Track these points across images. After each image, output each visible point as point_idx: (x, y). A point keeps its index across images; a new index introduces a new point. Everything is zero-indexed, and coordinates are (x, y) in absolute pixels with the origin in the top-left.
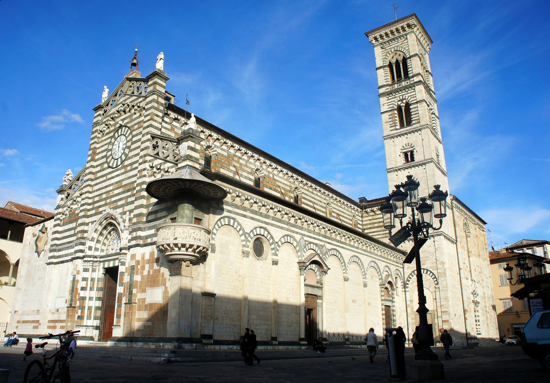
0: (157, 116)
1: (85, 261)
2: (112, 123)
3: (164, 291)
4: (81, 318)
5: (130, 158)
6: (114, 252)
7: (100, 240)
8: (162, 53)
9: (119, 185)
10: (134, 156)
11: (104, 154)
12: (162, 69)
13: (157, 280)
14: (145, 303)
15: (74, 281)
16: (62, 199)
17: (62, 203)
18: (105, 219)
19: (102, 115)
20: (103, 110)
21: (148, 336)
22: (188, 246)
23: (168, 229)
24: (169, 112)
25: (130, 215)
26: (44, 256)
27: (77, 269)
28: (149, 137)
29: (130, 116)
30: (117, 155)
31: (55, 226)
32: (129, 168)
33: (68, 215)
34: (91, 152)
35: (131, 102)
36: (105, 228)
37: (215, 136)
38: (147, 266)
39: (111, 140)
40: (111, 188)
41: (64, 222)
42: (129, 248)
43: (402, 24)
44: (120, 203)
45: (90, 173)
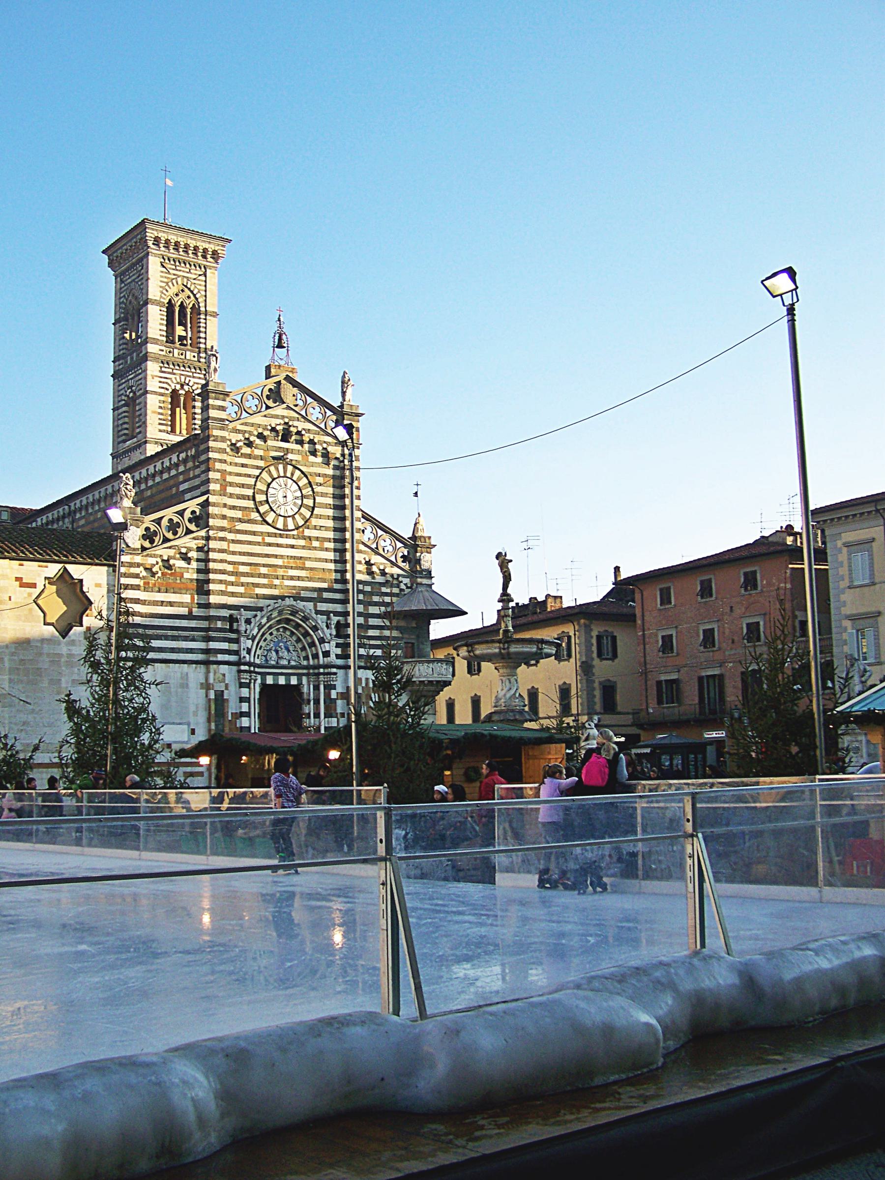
1: (239, 671)
5: (315, 528)
6: (285, 662)
32: (316, 544)
34: (217, 476)
35: (309, 431)
39: (261, 473)
40: (279, 562)
43: (207, 246)
45: (224, 517)
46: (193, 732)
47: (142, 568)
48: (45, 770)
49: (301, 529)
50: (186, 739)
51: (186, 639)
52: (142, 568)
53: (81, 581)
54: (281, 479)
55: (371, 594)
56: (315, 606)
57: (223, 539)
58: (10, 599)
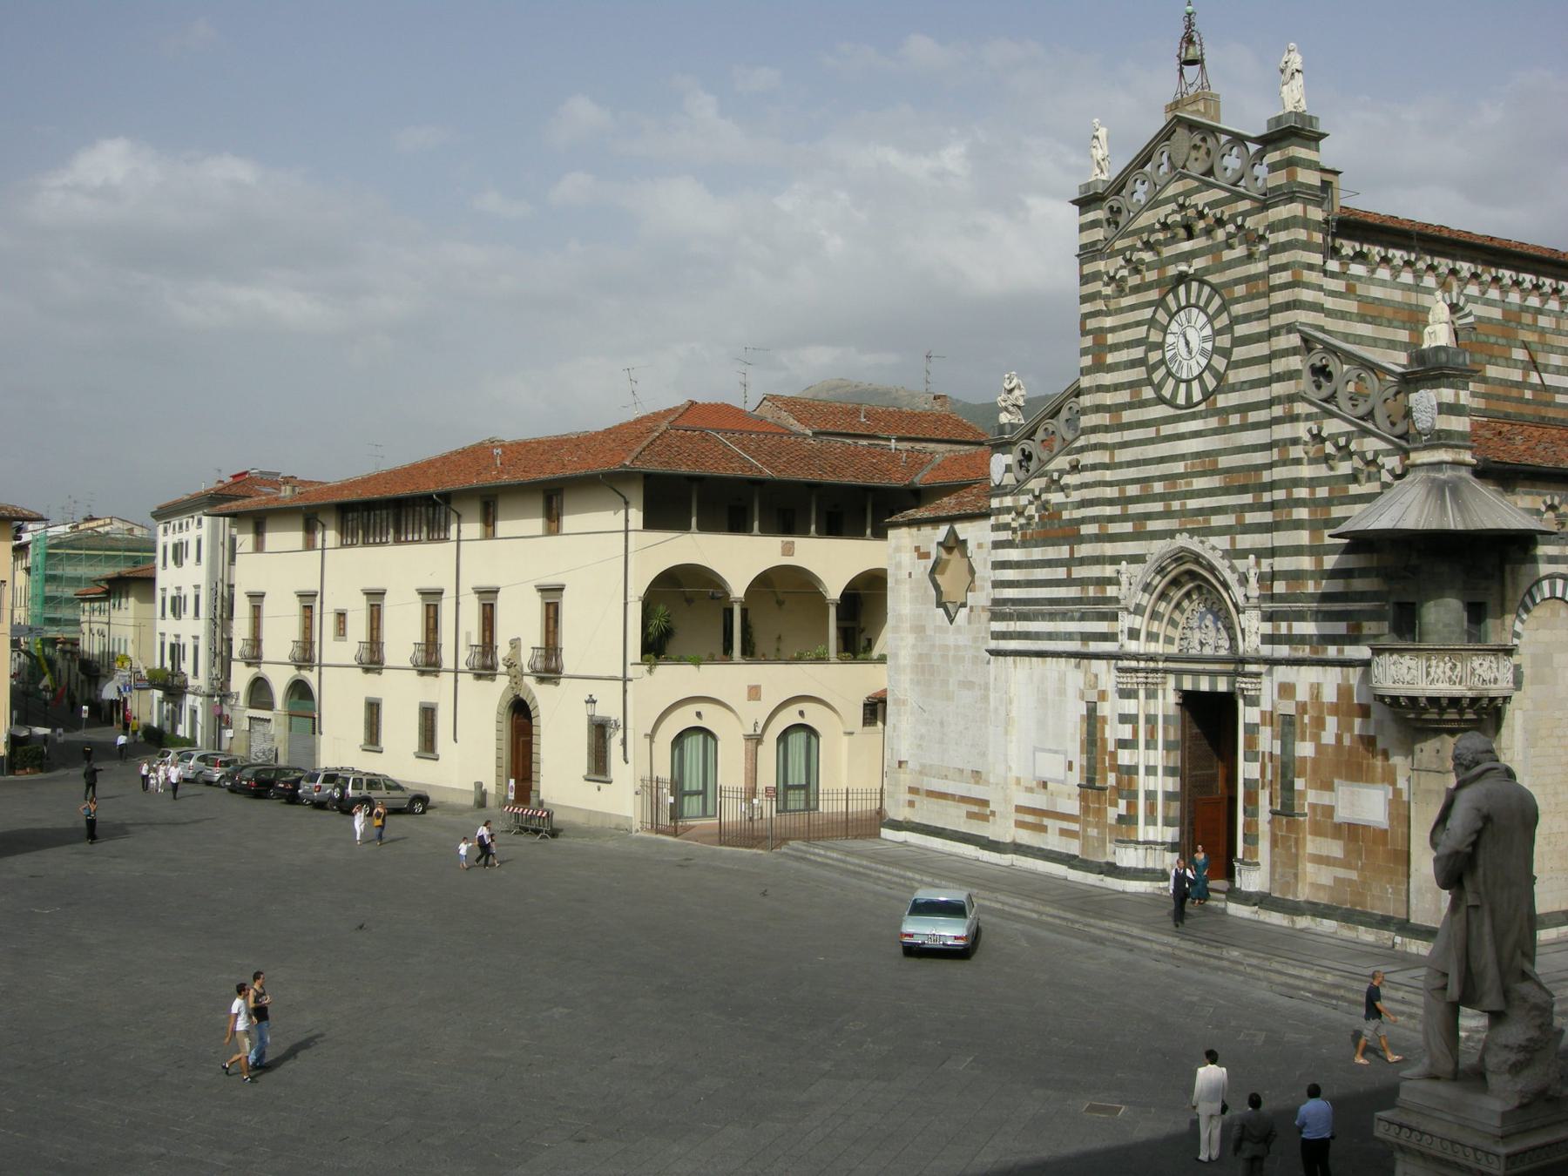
0: (1311, 267)
1: (1120, 670)
2: (1148, 256)
3: (1391, 797)
4: (1128, 820)
5: (1233, 388)
6: (1208, 651)
7: (1161, 610)
8: (1292, 45)
9: (1208, 467)
10: (1245, 386)
11: (1138, 353)
12: (1303, 107)
13: (1368, 764)
14: (1331, 816)
15: (1092, 719)
16: (1008, 469)
17: (1009, 479)
18: (1176, 560)
19: (1105, 224)
20: (1106, 205)
21: (1349, 906)
22: (1465, 703)
23: (1407, 657)
24: (1338, 242)
25: (1258, 564)
26: (969, 622)
27: (1099, 688)
28: (1295, 340)
29: (1213, 250)
30: (1185, 368)
31: (997, 545)
32: (1235, 420)
33: (1037, 519)
34: (1088, 341)
35: (1211, 205)
36: (1176, 583)
37: (1465, 268)
38: (1331, 722)
39: (1155, 312)
40: (1179, 467)
41: (1024, 535)
42: (1273, 662)
44: (1217, 521)
45: (1098, 409)
46: (1070, 766)
47: (1013, 514)
48: (935, 800)
49: (1212, 398)
50: (1063, 778)
51: (1065, 617)
52: (1013, 514)
53: (965, 542)
54: (1182, 313)
55: (1328, 502)
56: (1233, 542)
57: (1095, 447)
58: (910, 574)
